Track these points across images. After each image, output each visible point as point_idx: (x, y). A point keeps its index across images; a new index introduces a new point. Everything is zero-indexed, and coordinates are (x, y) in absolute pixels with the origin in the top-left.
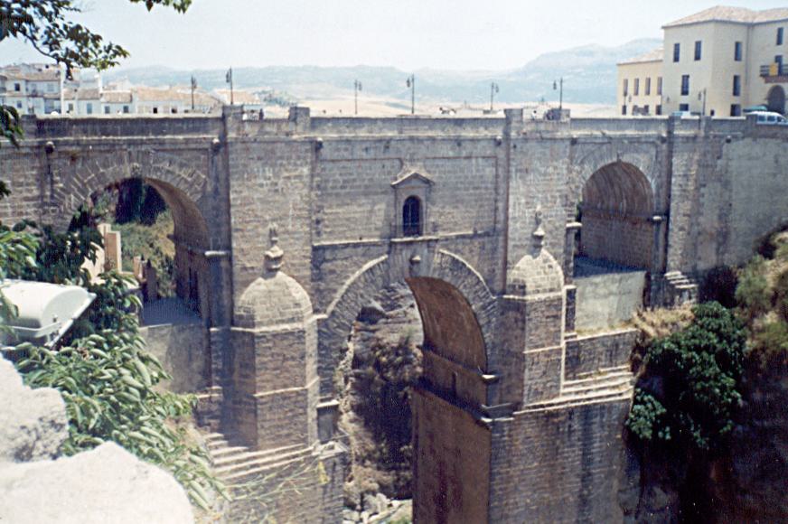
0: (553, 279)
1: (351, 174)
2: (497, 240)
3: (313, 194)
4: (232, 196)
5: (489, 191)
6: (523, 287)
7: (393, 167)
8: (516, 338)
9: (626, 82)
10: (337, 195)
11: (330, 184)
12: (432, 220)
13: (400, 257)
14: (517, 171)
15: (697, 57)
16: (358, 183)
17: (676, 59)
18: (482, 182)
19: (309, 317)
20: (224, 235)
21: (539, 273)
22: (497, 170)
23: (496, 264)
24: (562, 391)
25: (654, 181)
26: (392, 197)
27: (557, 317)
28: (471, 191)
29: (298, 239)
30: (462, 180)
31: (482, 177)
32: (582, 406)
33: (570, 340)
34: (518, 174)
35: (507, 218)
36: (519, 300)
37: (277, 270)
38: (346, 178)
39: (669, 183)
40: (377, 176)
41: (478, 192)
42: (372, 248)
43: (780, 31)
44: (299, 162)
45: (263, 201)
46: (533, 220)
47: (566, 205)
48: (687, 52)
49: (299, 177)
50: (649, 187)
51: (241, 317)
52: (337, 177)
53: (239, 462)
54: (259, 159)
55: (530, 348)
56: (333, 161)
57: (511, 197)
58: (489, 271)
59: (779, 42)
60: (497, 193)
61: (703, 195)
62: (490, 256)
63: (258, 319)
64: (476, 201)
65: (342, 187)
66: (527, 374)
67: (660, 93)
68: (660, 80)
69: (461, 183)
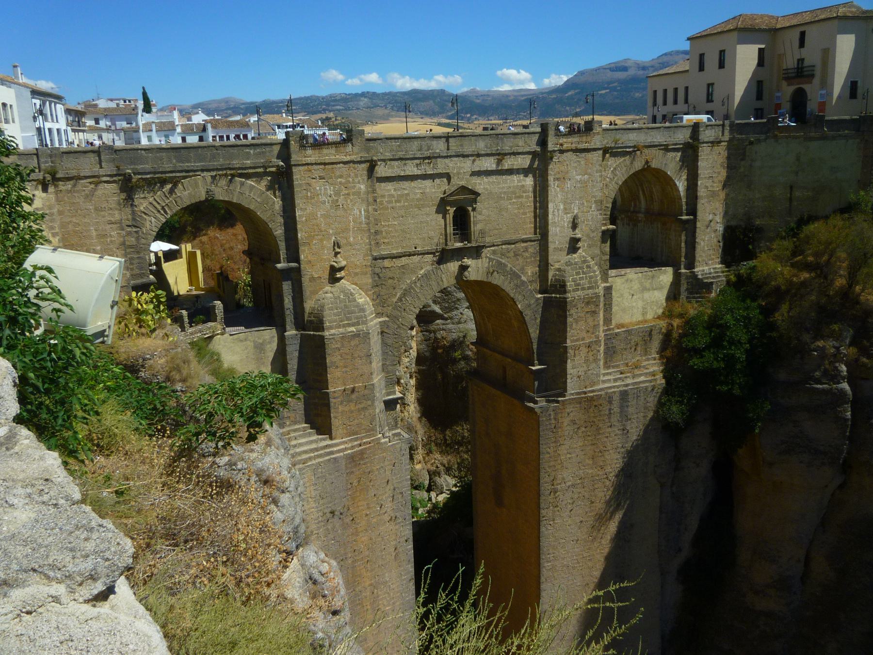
0: (591, 277)
3: (370, 208)
9: (655, 92)
12: (479, 227)
14: (554, 181)
15: (721, 65)
16: (412, 196)
17: (701, 68)
18: (524, 192)
19: (372, 320)
21: (578, 274)
24: (602, 378)
25: (681, 184)
27: (594, 313)
29: (359, 250)
31: (523, 186)
32: (621, 391)
33: (608, 333)
34: (557, 183)
36: (560, 297)
37: (341, 278)
40: (428, 190)
43: (803, 34)
45: (325, 216)
47: (601, 210)
48: (711, 61)
49: (358, 193)
50: (677, 190)
51: (311, 322)
53: (316, 450)
54: (321, 178)
55: (572, 342)
58: (533, 273)
59: (802, 44)
62: (533, 259)
63: (327, 324)
64: (519, 209)
65: (396, 201)
66: (569, 364)
67: (686, 101)
68: (687, 88)
69: (505, 193)
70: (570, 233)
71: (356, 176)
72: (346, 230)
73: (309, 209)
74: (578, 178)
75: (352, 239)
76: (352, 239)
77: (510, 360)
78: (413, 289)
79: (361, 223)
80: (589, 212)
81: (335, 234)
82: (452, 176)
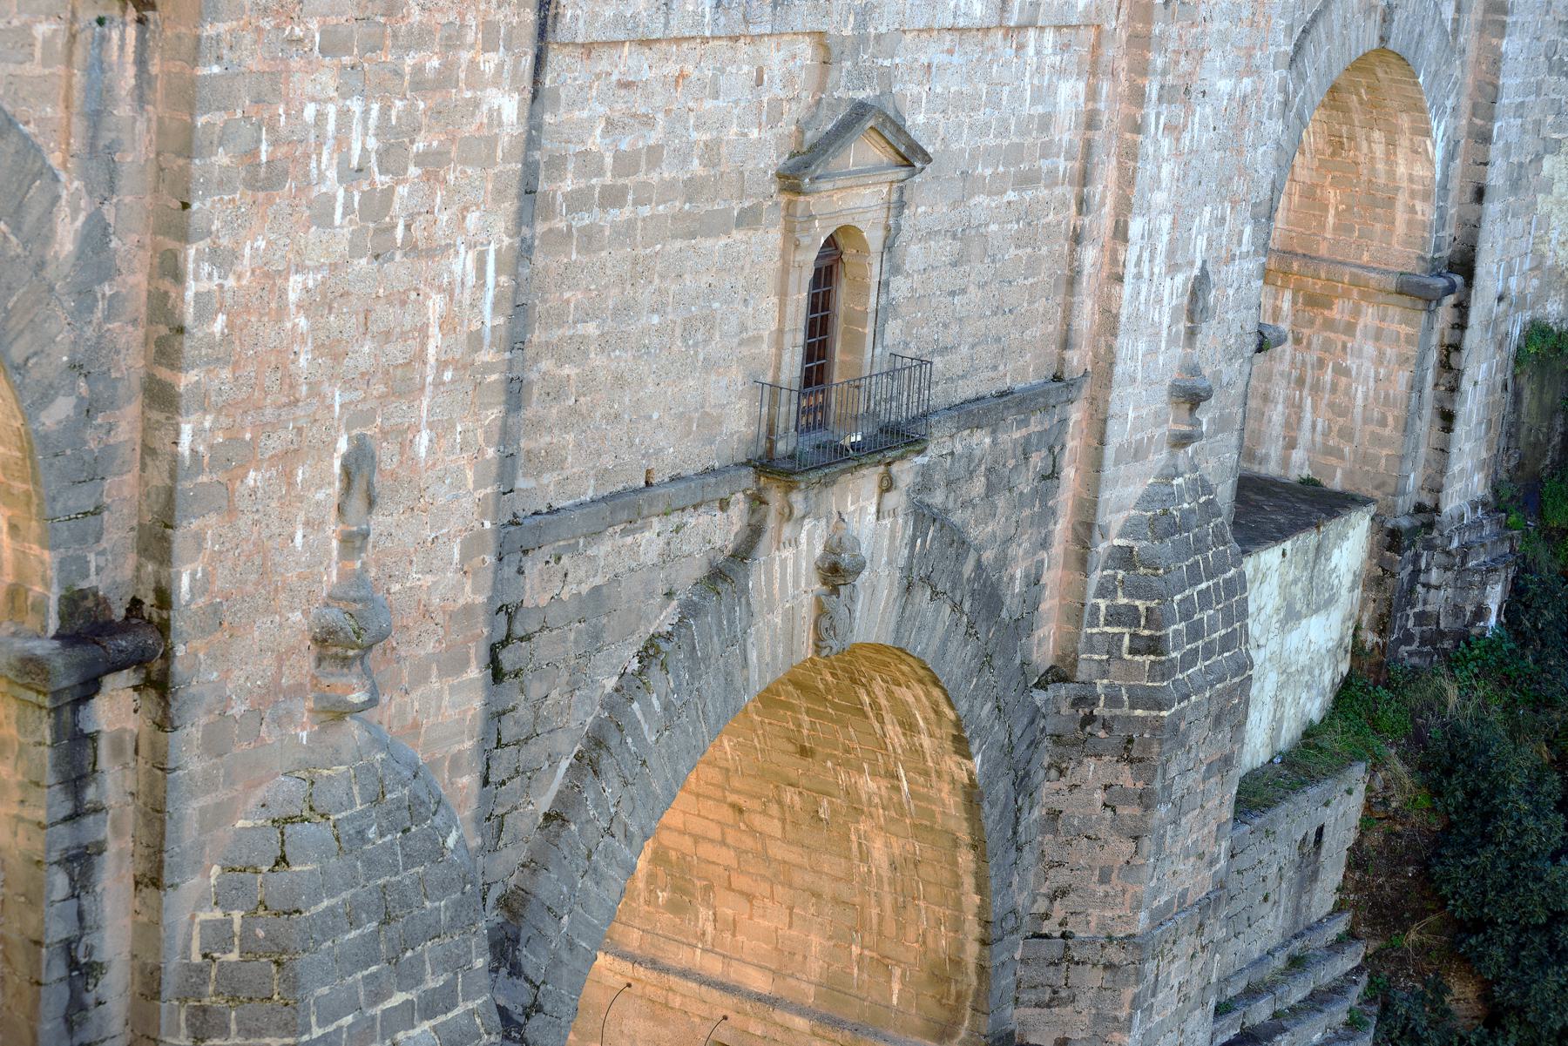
1: (647, 121)
2: (1063, 421)
4: (192, 288)
5: (1058, 191)
6: (1154, 646)
7: (789, 79)
8: (1104, 878)
10: (589, 239)
11: (568, 185)
13: (788, 553)
20: (118, 532)
22: (1092, 94)
23: (1045, 544)
26: (774, 237)
28: (1011, 195)
30: (990, 141)
35: (1110, 323)
38: (624, 146)
39: (1485, 138)
40: (734, 129)
41: (1028, 195)
42: (691, 520)
44: (489, 62)
45: (320, 303)
46: (1182, 326)
49: (480, 150)
52: (596, 141)
54: (332, 45)
56: (588, 48)
57: (1136, 227)
60: (1082, 204)
61: (1547, 188)
65: (612, 197)
70: (1168, 361)
71: (489, 29)
72: (402, 385)
73: (254, 246)
74: (1224, 85)
75: (423, 439)
76: (423, 439)
77: (800, 1023)
78: (636, 725)
79: (475, 341)
80: (1233, 258)
81: (358, 417)
82: (836, 51)
